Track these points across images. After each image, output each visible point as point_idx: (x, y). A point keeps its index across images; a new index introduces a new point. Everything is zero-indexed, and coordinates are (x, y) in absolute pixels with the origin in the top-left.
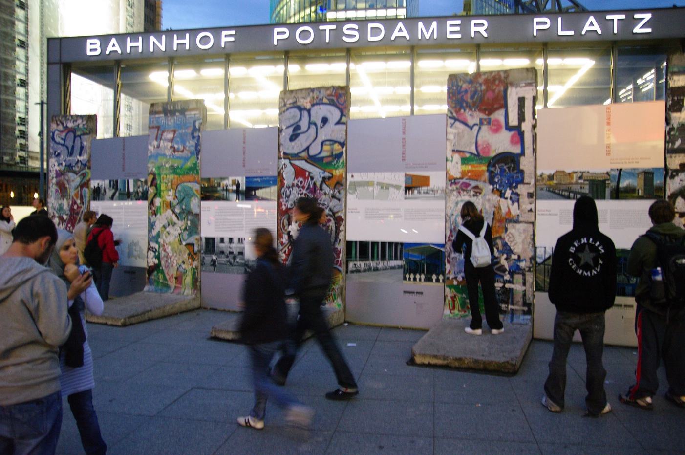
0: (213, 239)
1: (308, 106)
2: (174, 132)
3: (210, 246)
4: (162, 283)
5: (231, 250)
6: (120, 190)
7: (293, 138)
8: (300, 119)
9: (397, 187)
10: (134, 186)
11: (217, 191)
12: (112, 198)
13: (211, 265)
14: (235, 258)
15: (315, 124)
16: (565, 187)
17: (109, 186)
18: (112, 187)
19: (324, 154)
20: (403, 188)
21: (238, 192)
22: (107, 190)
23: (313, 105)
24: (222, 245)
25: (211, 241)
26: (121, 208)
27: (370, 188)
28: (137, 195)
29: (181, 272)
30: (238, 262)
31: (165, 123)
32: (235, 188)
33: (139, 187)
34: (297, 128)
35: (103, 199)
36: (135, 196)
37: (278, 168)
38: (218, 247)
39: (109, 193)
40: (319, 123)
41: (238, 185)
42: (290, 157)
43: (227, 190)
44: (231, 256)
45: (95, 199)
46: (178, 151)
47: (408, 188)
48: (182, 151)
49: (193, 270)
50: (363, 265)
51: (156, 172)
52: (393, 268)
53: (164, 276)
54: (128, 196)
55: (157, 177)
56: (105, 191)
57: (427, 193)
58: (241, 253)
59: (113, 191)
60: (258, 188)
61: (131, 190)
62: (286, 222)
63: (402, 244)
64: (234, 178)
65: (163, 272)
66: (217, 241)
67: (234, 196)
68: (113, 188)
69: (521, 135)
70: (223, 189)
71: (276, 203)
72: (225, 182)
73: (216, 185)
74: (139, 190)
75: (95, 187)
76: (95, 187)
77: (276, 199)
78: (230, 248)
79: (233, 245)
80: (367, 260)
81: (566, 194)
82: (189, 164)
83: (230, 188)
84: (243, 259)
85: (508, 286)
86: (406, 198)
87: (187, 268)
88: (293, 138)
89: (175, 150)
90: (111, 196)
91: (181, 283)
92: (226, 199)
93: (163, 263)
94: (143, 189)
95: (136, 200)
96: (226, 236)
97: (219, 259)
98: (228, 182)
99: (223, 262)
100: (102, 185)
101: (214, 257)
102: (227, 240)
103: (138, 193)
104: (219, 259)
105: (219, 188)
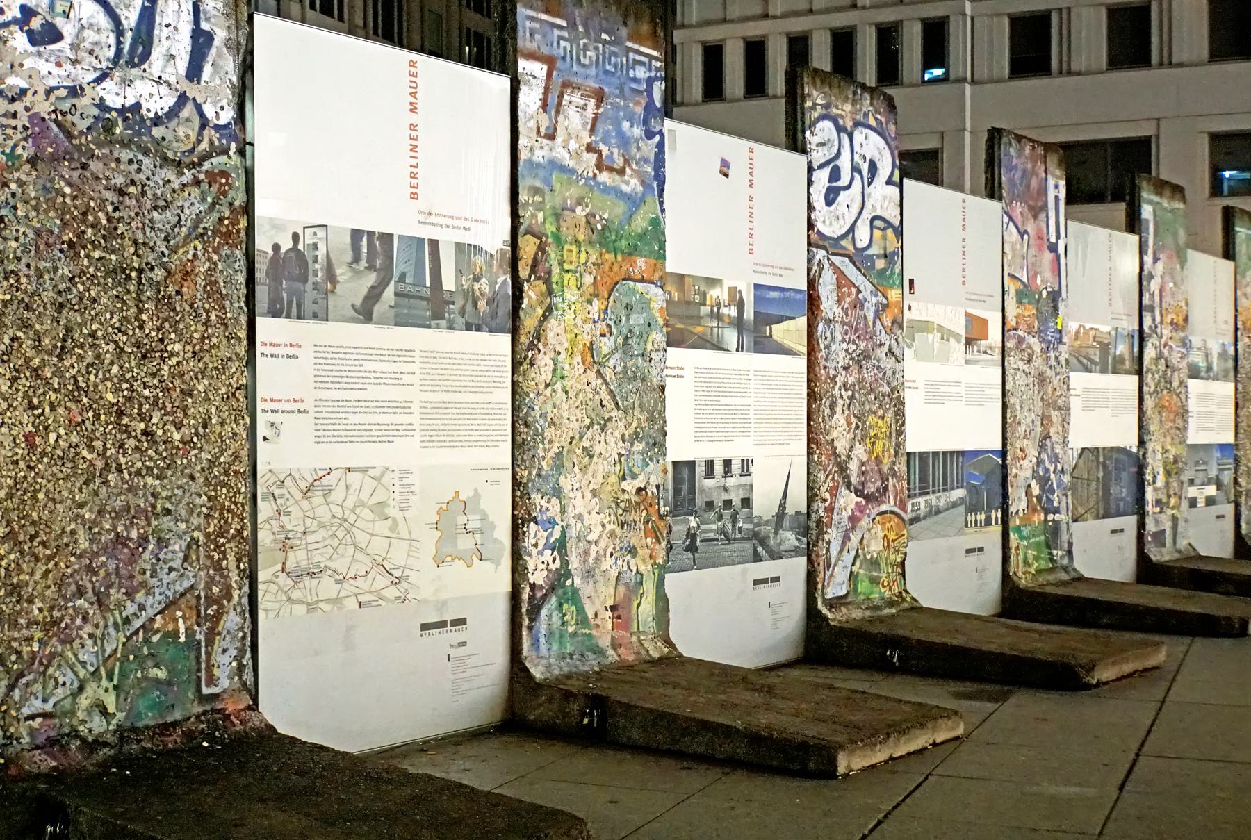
0: (691, 464)
1: (849, 124)
2: (600, 97)
3: (685, 488)
4: (574, 634)
5: (726, 497)
6: (402, 278)
7: (831, 196)
8: (838, 154)
9: (957, 337)
10: (459, 272)
11: (698, 319)
12: (365, 313)
13: (686, 550)
14: (734, 519)
15: (860, 173)
16: (1084, 352)
17: (349, 257)
18: (363, 264)
19: (874, 250)
20: (963, 341)
21: (739, 323)
22: (341, 272)
23: (857, 124)
24: (710, 483)
25: (685, 473)
26: (405, 355)
27: (930, 337)
28: (469, 307)
29: (627, 585)
30: (740, 528)
31: (571, 52)
32: (733, 312)
33: (477, 279)
34: (835, 174)
35: (321, 315)
36: (462, 313)
37: (809, 270)
38: (702, 491)
39: (353, 287)
40: (865, 168)
41: (741, 306)
42: (826, 244)
43: (719, 317)
44: (727, 513)
45: (275, 312)
46: (611, 169)
47: (969, 342)
48: (621, 172)
49: (656, 572)
50: (923, 503)
51: (550, 228)
52: (955, 505)
53: (581, 610)
54: (432, 307)
55: (552, 251)
56: (331, 276)
57: (985, 353)
58: (746, 503)
59: (371, 279)
60: (781, 319)
61: (449, 283)
62: (827, 411)
63: (963, 453)
64: (732, 284)
65: (574, 597)
66: (700, 470)
67: (731, 337)
68: (371, 267)
69: (1058, 258)
70: (711, 315)
71: (802, 363)
72: (715, 293)
73: (697, 299)
74: (476, 286)
75: (276, 247)
76: (276, 247)
77: (805, 350)
78: (726, 490)
79: (731, 482)
80: (927, 493)
81: (1085, 361)
82: (641, 222)
83: (725, 311)
84: (749, 519)
85: (1057, 517)
86: (967, 362)
87: (642, 568)
88: (831, 196)
89: (600, 166)
90: (358, 302)
91: (626, 626)
92: (718, 347)
93: (575, 563)
94: (492, 284)
95: (468, 328)
96: (717, 452)
97: (703, 527)
98: (719, 294)
99: (711, 535)
100: (315, 246)
101: (693, 523)
102: (718, 468)
103: (475, 304)
104: (703, 527)
105: (704, 310)
